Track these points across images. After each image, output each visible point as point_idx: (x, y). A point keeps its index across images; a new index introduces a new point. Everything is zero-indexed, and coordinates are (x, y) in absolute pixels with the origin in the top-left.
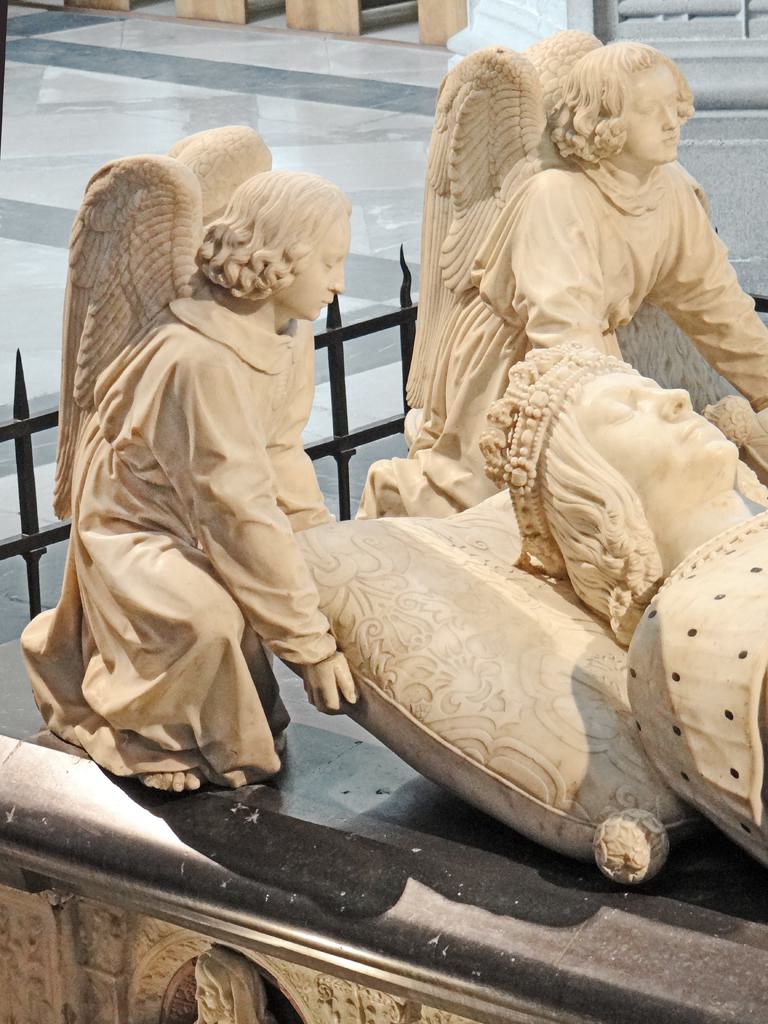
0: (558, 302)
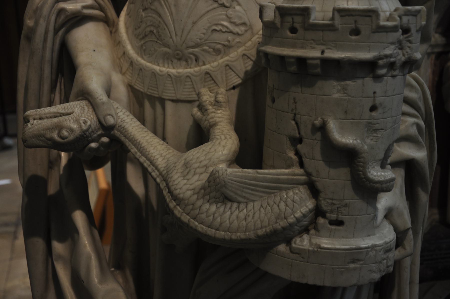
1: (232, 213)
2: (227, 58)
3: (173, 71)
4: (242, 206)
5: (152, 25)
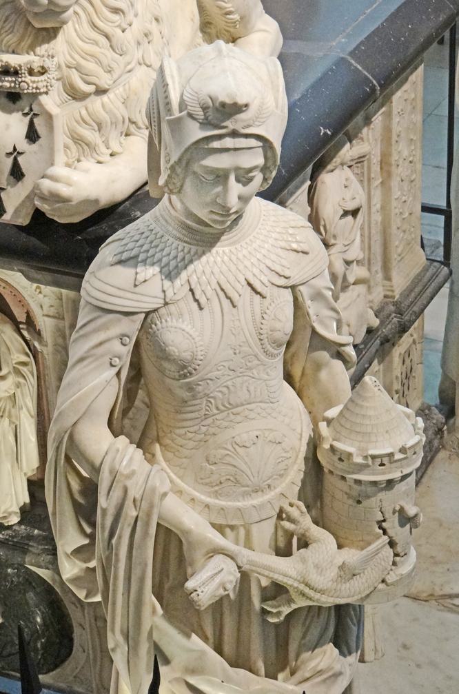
1: (358, 583)
2: (289, 478)
3: (255, 502)
4: (362, 575)
5: (227, 475)
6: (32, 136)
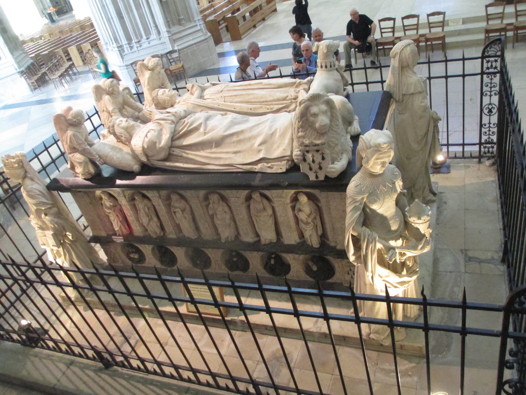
0: (112, 110)
6: (323, 158)
